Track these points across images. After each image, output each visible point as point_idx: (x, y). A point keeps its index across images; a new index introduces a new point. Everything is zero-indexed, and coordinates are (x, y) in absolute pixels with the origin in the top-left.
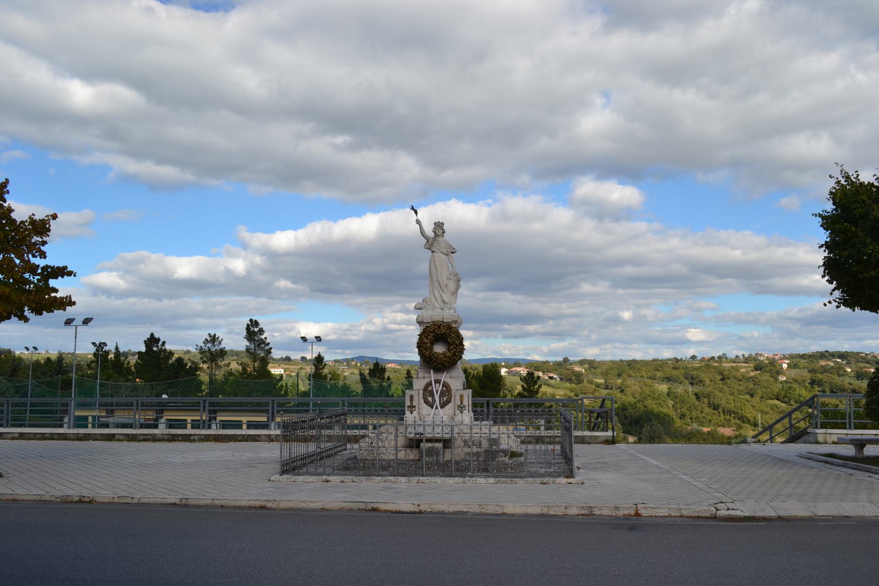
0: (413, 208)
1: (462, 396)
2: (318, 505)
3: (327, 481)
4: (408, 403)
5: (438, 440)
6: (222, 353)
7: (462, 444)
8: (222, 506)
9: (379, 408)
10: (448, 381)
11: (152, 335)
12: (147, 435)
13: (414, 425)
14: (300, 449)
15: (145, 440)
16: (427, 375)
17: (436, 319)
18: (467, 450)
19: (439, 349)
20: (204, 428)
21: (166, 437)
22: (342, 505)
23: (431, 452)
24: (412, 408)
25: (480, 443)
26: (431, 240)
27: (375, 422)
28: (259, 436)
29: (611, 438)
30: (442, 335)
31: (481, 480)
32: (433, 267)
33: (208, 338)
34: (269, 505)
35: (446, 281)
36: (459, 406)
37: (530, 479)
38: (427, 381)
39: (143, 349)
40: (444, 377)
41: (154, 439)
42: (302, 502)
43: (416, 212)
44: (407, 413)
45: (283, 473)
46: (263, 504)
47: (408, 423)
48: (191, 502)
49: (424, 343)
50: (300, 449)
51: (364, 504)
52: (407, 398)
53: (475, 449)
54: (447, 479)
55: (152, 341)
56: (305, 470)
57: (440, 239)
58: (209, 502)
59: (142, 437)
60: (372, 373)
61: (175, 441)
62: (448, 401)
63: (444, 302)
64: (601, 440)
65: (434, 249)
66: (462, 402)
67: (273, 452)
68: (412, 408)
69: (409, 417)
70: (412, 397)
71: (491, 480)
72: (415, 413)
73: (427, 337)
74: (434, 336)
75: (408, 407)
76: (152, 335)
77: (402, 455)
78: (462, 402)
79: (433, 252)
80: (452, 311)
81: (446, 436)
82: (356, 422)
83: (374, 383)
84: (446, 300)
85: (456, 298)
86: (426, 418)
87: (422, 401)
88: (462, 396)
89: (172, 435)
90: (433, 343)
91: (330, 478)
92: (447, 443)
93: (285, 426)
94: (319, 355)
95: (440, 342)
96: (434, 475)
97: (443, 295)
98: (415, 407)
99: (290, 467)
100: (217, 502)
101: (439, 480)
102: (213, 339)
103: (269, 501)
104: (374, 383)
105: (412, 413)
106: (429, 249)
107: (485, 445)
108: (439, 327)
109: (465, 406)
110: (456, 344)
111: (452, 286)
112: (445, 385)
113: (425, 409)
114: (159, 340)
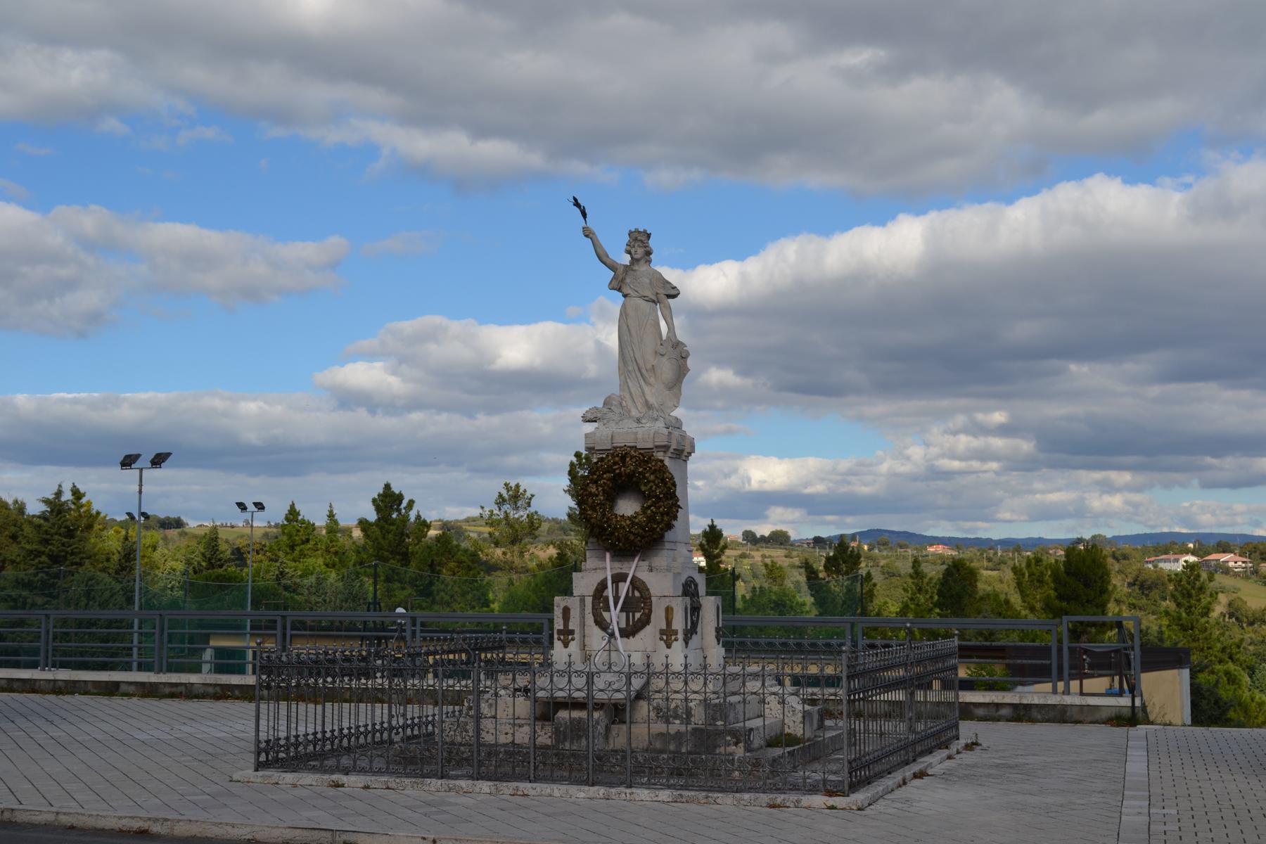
0: (577, 204)
1: (669, 611)
2: (244, 833)
3: (337, 785)
4: (559, 624)
5: (599, 706)
6: (533, 524)
7: (652, 714)
8: (72, 828)
9: (518, 637)
10: (644, 575)
11: (387, 486)
12: (177, 685)
13: (568, 672)
14: (306, 720)
15: (172, 696)
16: (598, 564)
17: (620, 442)
18: (659, 727)
19: (627, 507)
20: (160, 671)
21: (211, 690)
22: (289, 834)
23: (578, 730)
24: (567, 634)
25: (689, 713)
26: (621, 270)
27: (797, 670)
28: (117, 684)
29: (1127, 713)
30: (631, 476)
31: (643, 794)
32: (625, 327)
33: (504, 493)
34: (156, 828)
35: (652, 360)
36: (662, 632)
37: (746, 796)
38: (598, 577)
39: (372, 516)
40: (633, 568)
41: (188, 693)
42: (216, 824)
43: (584, 215)
44: (558, 644)
45: (259, 766)
46: (145, 825)
47: (557, 667)
48: (21, 817)
49: (591, 495)
50: (306, 720)
51: (328, 834)
52: (558, 613)
53: (676, 726)
54: (573, 789)
55: (388, 501)
56: (330, 762)
57: (642, 268)
58: (51, 818)
59: (167, 690)
60: (831, 563)
61: (226, 697)
62: (645, 621)
63: (649, 406)
64: (1104, 715)
65: (627, 290)
66: (669, 623)
67: (237, 723)
68: (567, 634)
69: (559, 653)
70: (566, 612)
71: (665, 795)
72: (574, 647)
73: (595, 482)
74: (613, 480)
75: (559, 632)
76: (387, 486)
77: (523, 735)
78: (669, 623)
79: (625, 296)
80: (660, 425)
81: (576, 694)
82: (813, 670)
83: (837, 585)
84: (651, 400)
85: (678, 396)
86: (590, 654)
87: (590, 619)
88: (669, 611)
89: (223, 686)
90: (611, 499)
91: (344, 779)
92: (618, 712)
93: (266, 667)
94: (712, 527)
95: (628, 491)
96: (552, 780)
97: (646, 389)
98: (572, 632)
99: (275, 756)
100: (64, 820)
101: (557, 790)
102: (515, 496)
103: (156, 820)
104: (837, 585)
105: (566, 646)
106: (619, 290)
107: (699, 717)
108: (623, 458)
109: (676, 633)
110: (664, 500)
111: (666, 369)
112: (636, 584)
113: (596, 638)
114: (400, 497)
